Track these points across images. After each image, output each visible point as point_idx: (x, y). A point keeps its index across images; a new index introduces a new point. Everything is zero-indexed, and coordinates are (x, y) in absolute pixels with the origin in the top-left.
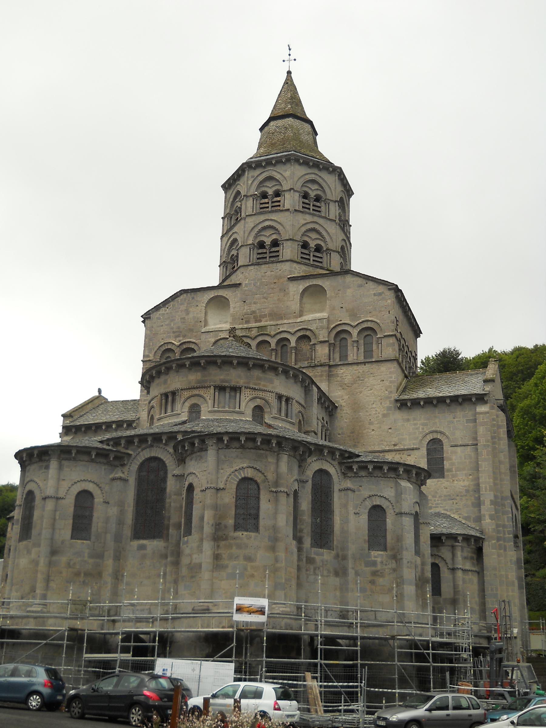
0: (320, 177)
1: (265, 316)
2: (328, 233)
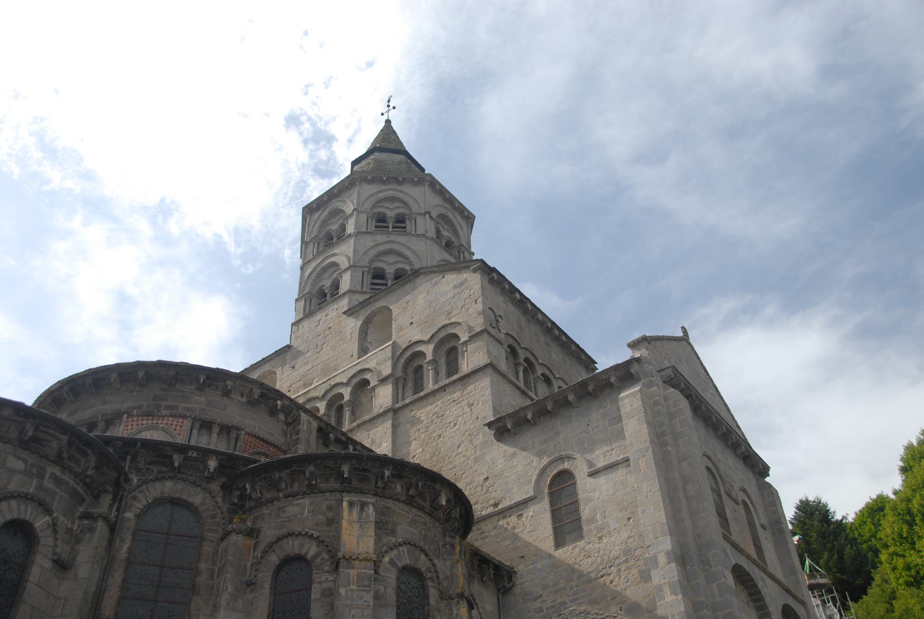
0: (401, 191)
2: (414, 252)
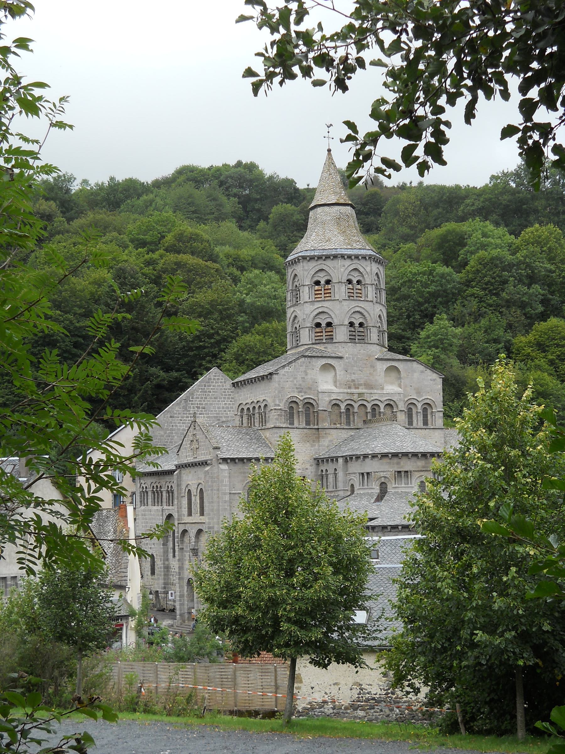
1: (361, 385)
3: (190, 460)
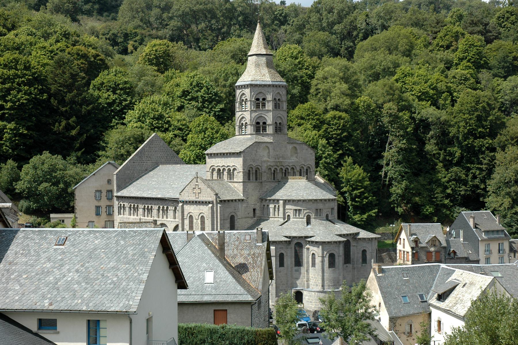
3: (193, 198)
